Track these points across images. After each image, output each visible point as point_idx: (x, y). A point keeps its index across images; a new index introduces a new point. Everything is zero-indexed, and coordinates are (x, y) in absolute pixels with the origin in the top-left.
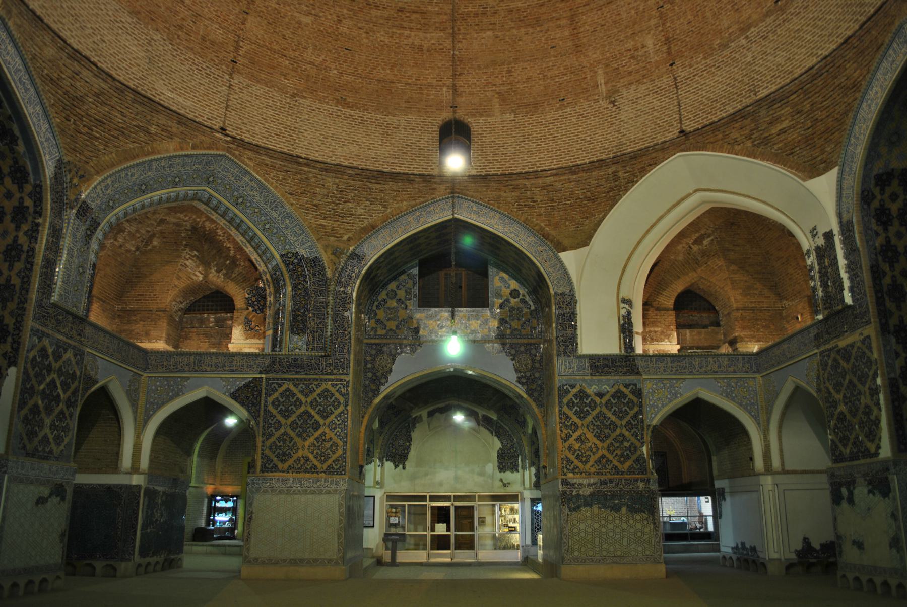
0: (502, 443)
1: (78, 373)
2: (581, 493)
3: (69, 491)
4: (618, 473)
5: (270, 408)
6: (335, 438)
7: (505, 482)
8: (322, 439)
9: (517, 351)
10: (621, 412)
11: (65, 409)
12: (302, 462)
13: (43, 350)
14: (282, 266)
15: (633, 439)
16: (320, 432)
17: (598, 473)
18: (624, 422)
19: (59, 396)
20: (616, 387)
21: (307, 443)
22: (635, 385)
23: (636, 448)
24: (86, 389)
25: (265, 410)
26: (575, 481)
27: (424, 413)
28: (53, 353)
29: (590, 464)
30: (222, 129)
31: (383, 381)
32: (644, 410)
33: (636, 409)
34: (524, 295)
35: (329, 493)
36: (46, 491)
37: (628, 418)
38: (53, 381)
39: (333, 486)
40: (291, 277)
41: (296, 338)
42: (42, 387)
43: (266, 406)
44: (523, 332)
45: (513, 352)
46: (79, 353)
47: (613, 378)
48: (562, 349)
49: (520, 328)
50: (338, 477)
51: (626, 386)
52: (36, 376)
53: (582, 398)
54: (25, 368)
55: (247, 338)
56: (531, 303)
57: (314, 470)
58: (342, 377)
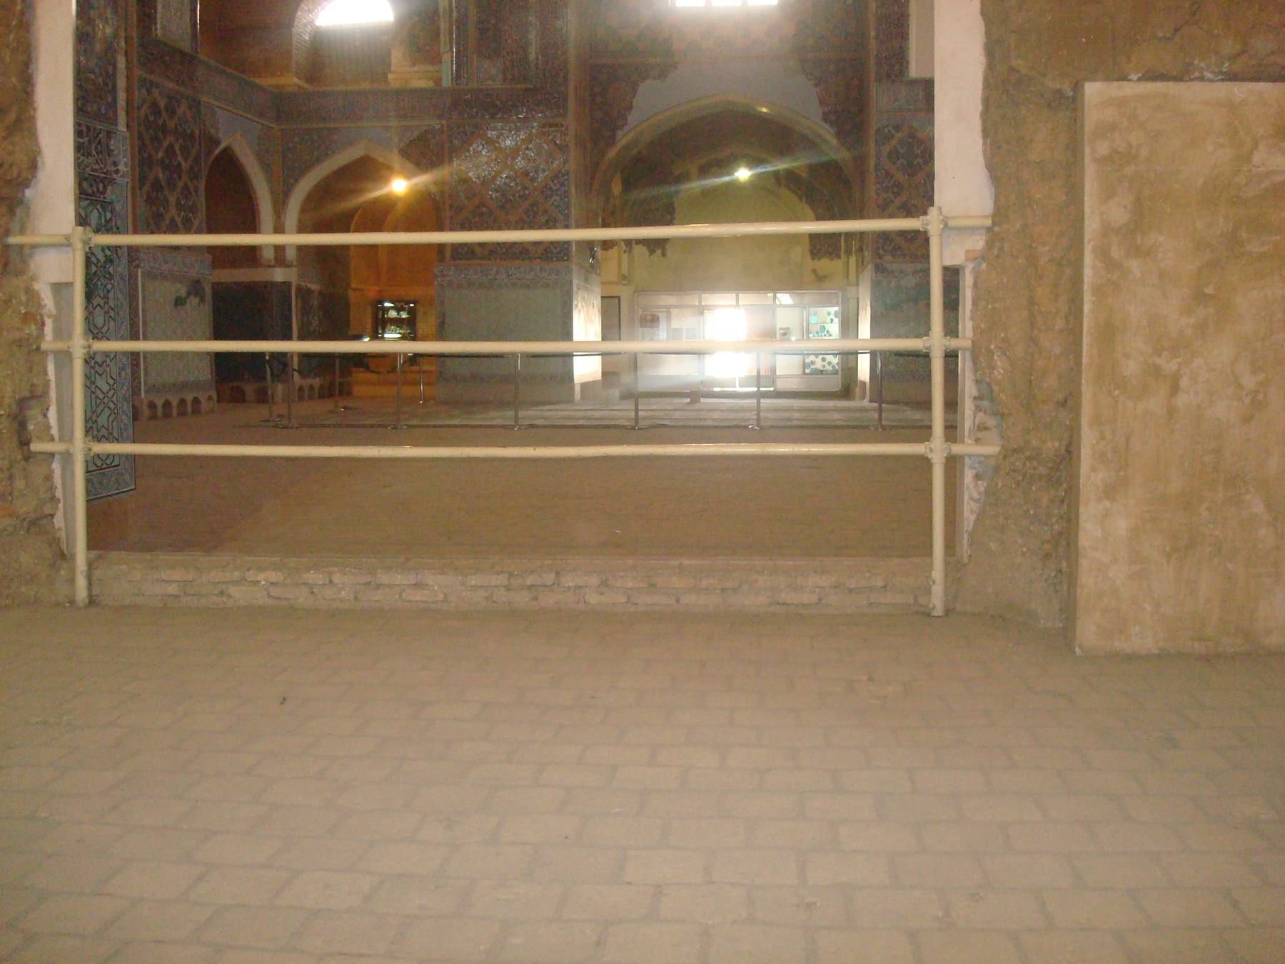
1: (197, 132)
3: (208, 290)
7: (820, 273)
11: (189, 183)
13: (155, 105)
19: (179, 165)
24: (209, 152)
28: (167, 109)
36: (183, 292)
38: (171, 146)
39: (554, 277)
41: (486, 64)
42: (160, 155)
46: (195, 104)
52: (152, 139)
54: (139, 133)
55: (414, 64)
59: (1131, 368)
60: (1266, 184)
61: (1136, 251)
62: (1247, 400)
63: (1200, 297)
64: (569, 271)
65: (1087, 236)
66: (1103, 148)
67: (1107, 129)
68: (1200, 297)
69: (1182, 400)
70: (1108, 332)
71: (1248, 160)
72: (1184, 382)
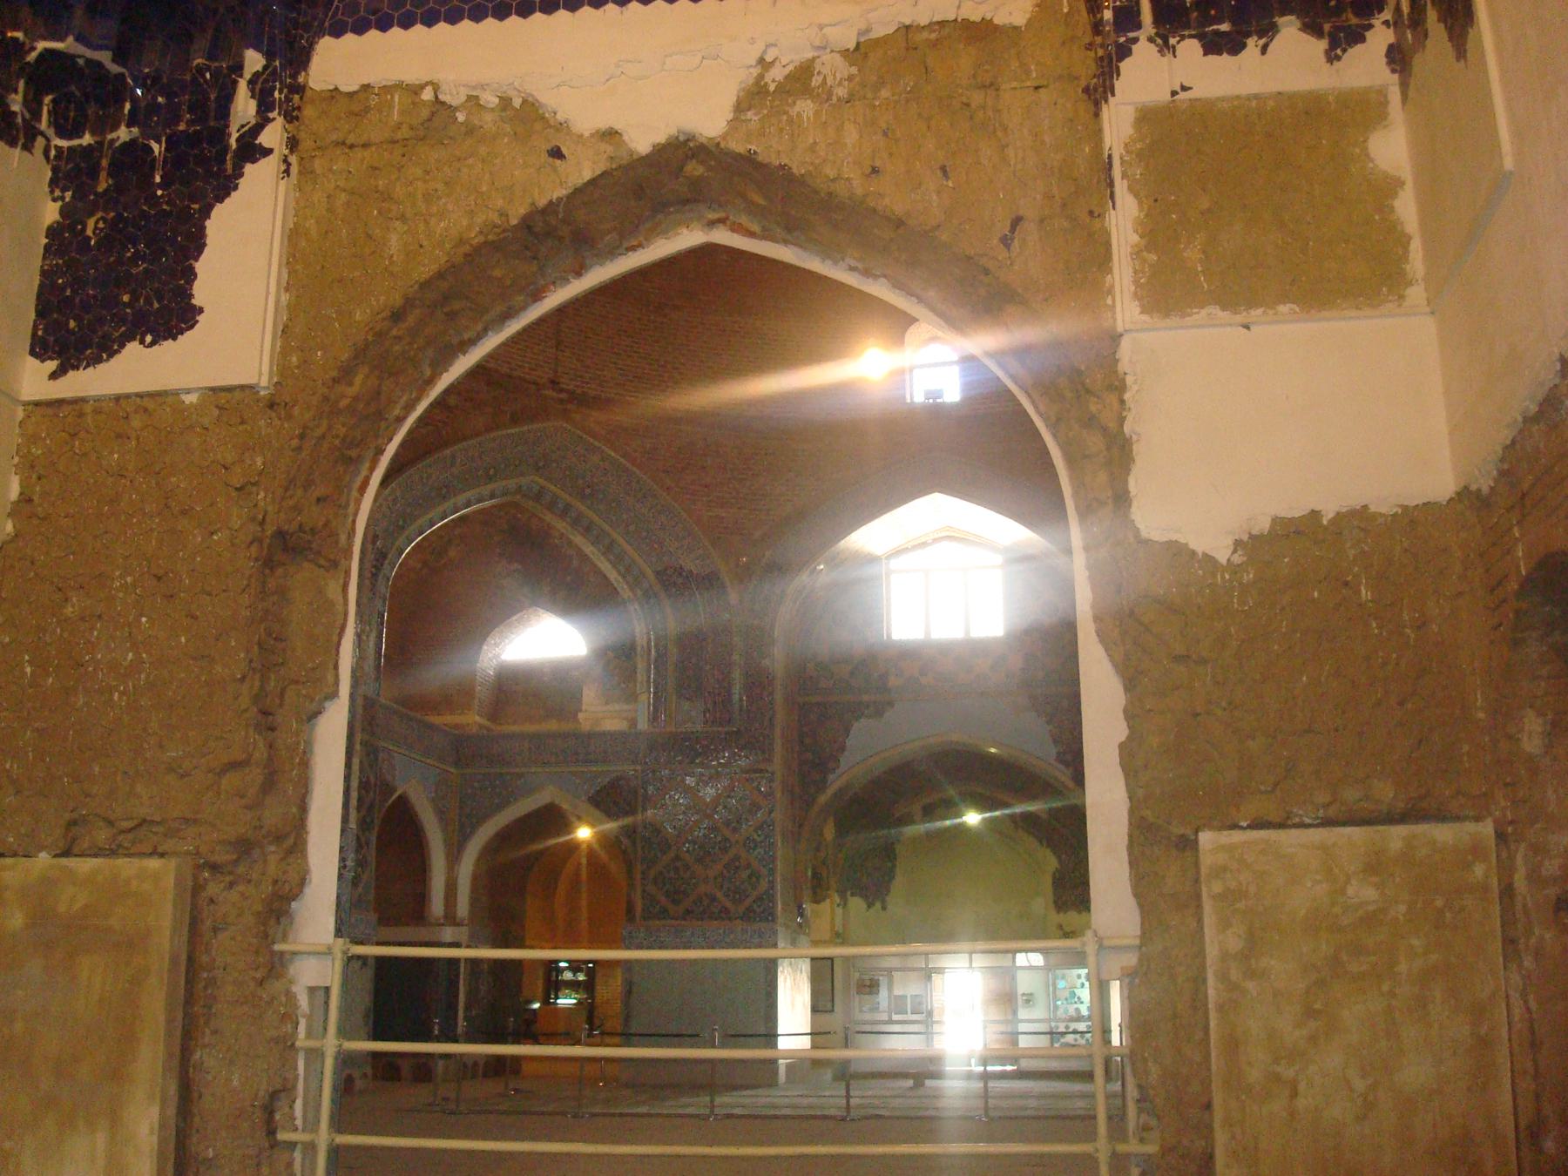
0: (1059, 858)
1: (372, 780)
7: (1067, 929)
27: (916, 808)
30: (553, 382)
41: (686, 705)
58: (762, 766)
59: (1254, 1075)
60: (1361, 912)
61: (1251, 974)
62: (1359, 1102)
63: (1310, 1013)
64: (775, 933)
65: (1209, 961)
66: (1217, 887)
67: (1219, 871)
68: (1310, 1013)
69: (1301, 1103)
70: (1233, 1045)
71: (1343, 892)
72: (1302, 1087)
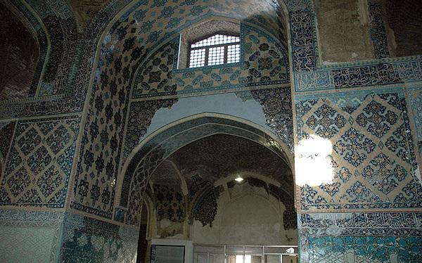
2: (328, 232)
4: (381, 206)
5: (16, 146)
6: (61, 171)
8: (50, 173)
9: (266, 96)
10: (379, 127)
12: (31, 194)
14: (45, 29)
15: (399, 160)
16: (50, 166)
17: (351, 206)
18: (384, 140)
20: (370, 99)
21: (38, 177)
22: (396, 95)
23: (404, 171)
25: (12, 148)
26: (320, 216)
29: (339, 194)
31: (143, 132)
32: (412, 123)
33: (399, 123)
34: (272, 47)
35: (46, 226)
37: (389, 134)
40: (51, 38)
43: (13, 144)
44: (273, 79)
45: (262, 97)
47: (363, 90)
48: (299, 63)
49: (269, 76)
50: (57, 210)
51: (384, 97)
53: (325, 115)
56: (280, 53)
57: (38, 202)
